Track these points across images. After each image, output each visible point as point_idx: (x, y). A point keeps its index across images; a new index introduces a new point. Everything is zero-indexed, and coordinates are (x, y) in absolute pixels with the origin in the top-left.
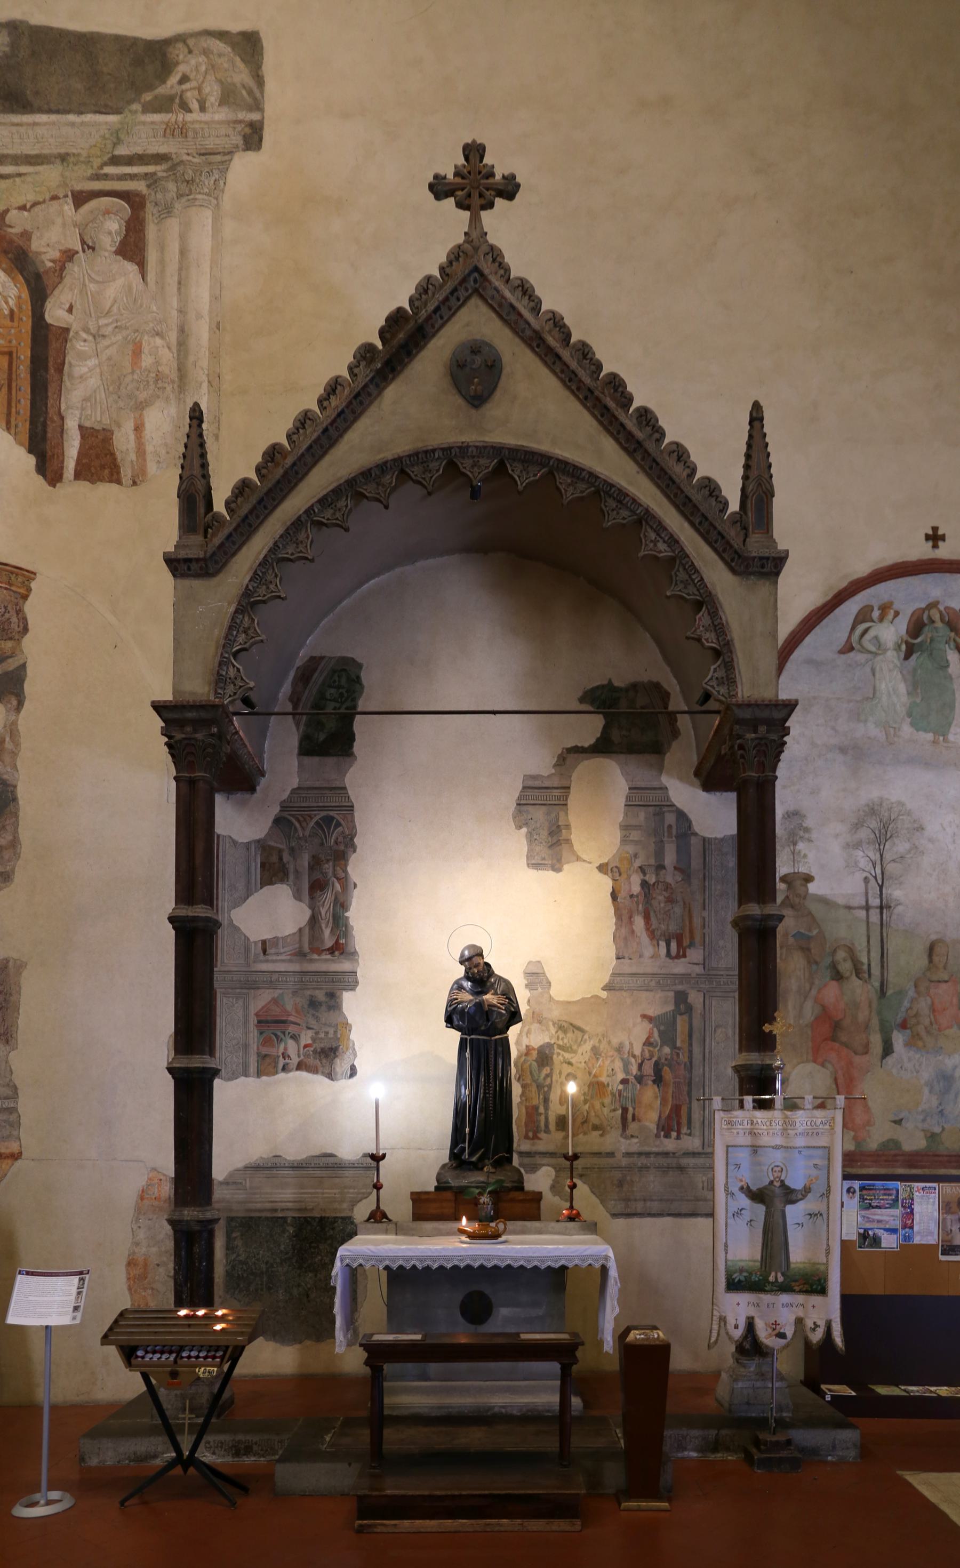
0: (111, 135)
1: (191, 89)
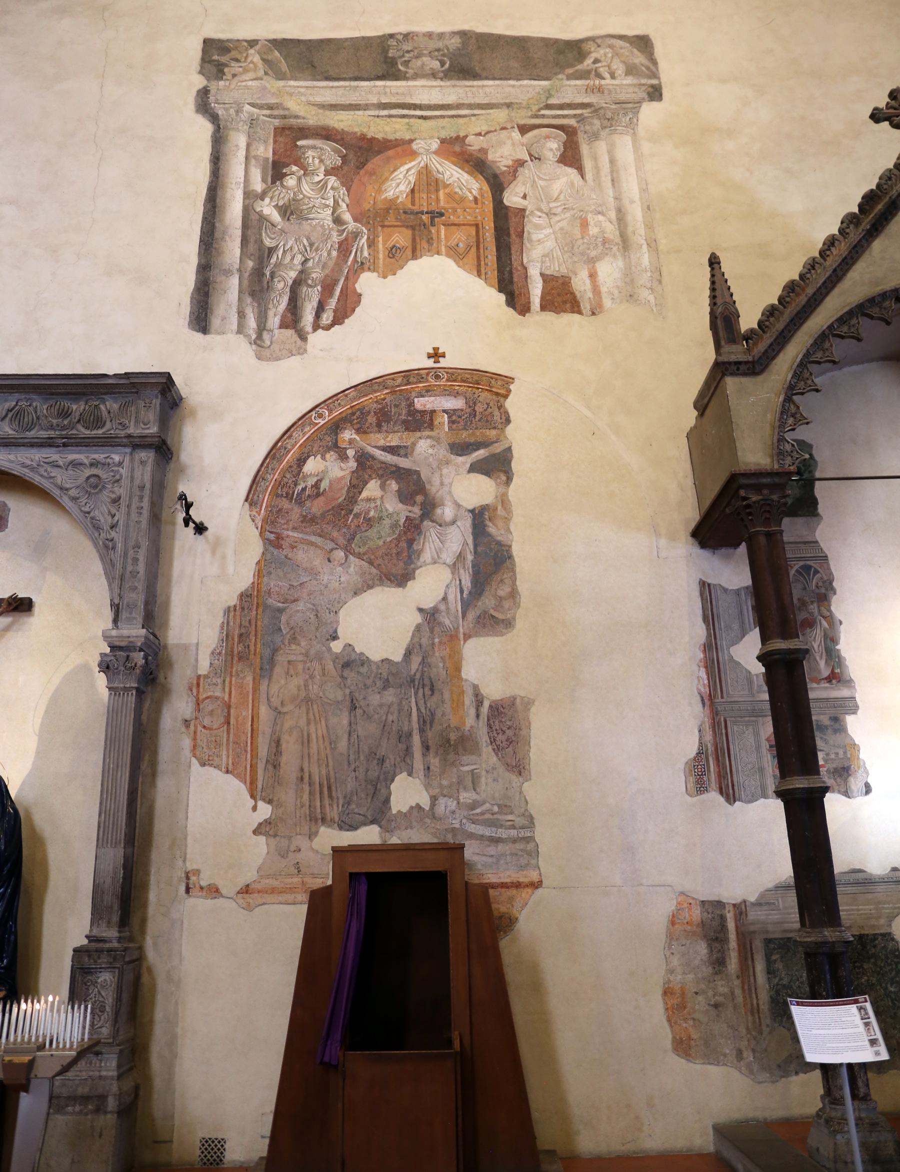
0: (545, 92)
1: (602, 66)
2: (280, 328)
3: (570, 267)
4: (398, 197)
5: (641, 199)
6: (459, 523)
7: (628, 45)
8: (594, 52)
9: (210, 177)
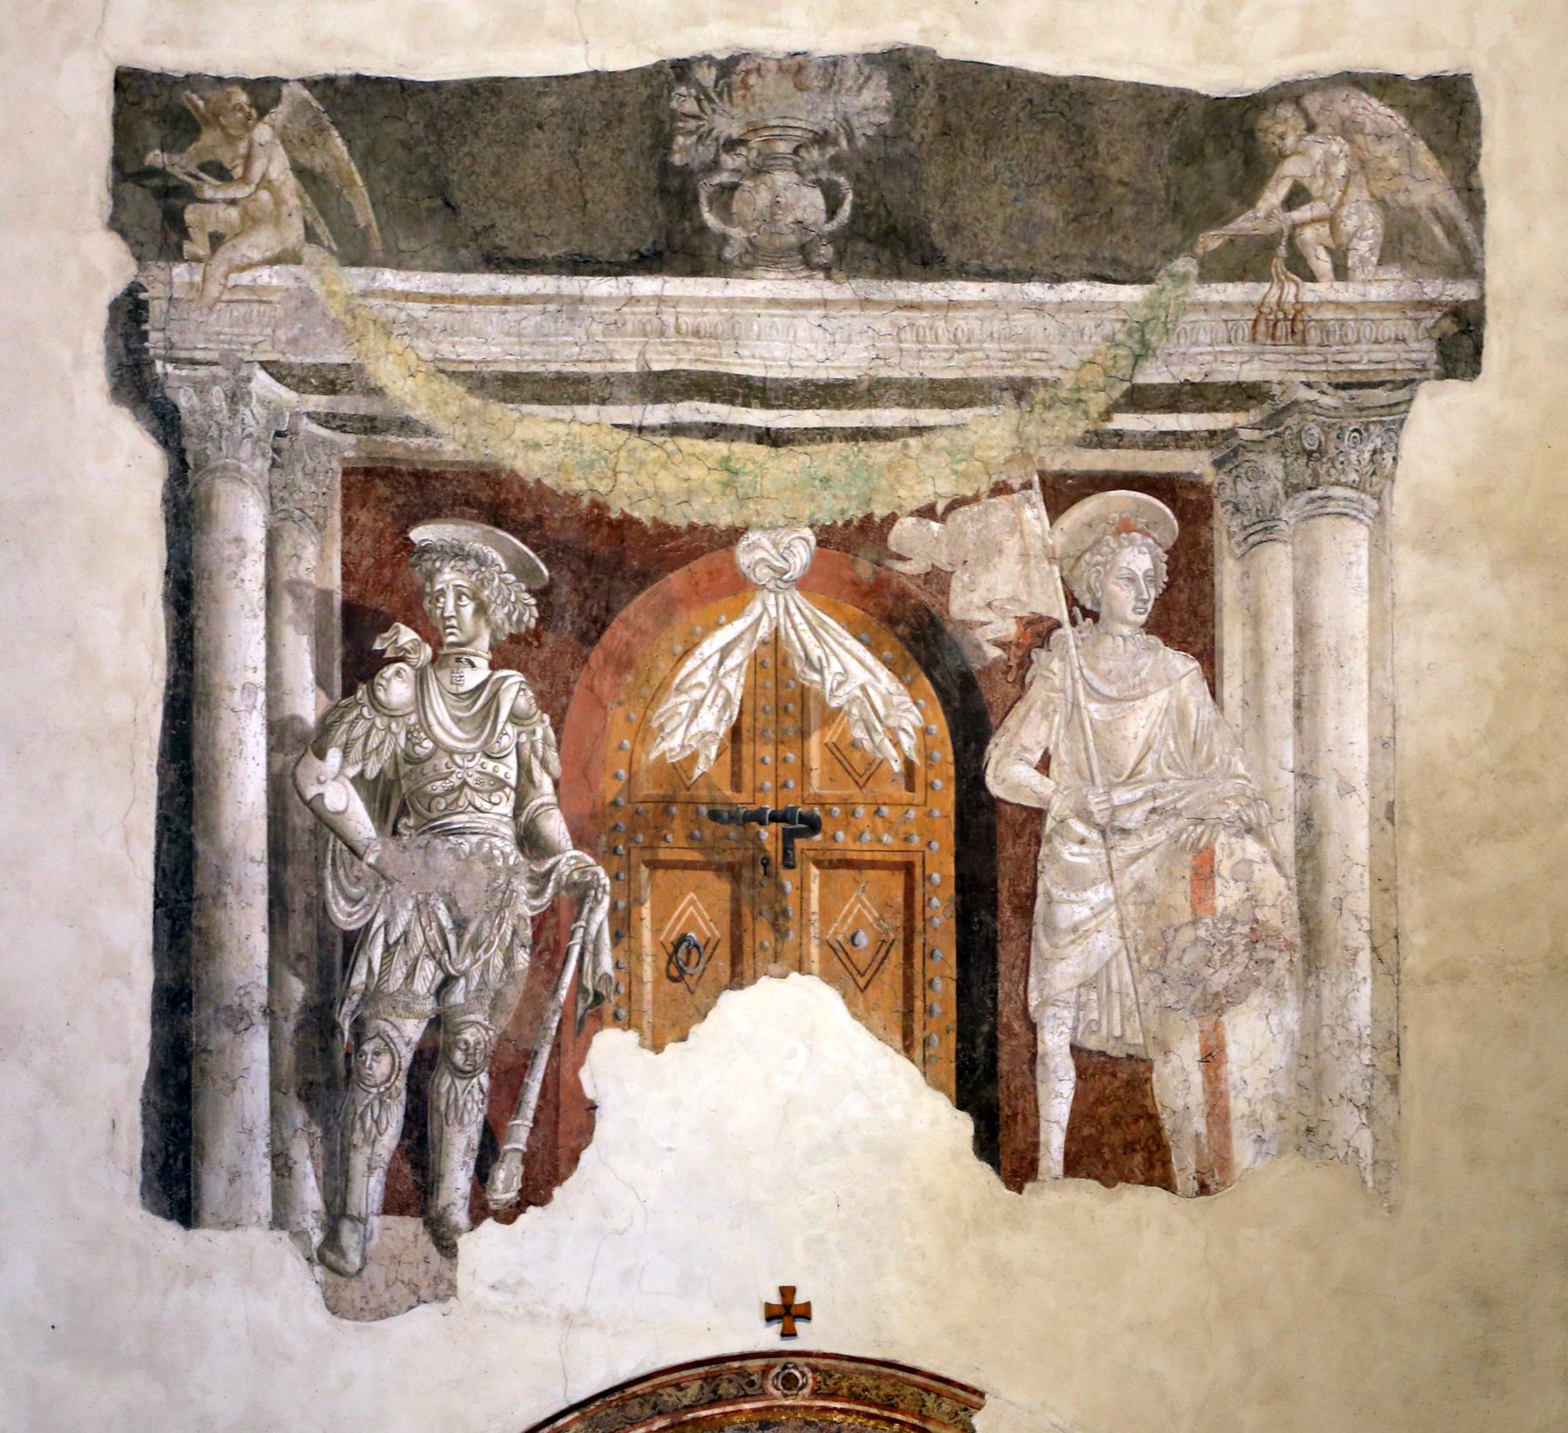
0: (1130, 334)
1: (1313, 221)
2: (386, 1211)
3: (1154, 1027)
4: (694, 758)
5: (1372, 779)
7: (1401, 121)
8: (1295, 153)
9: (170, 661)
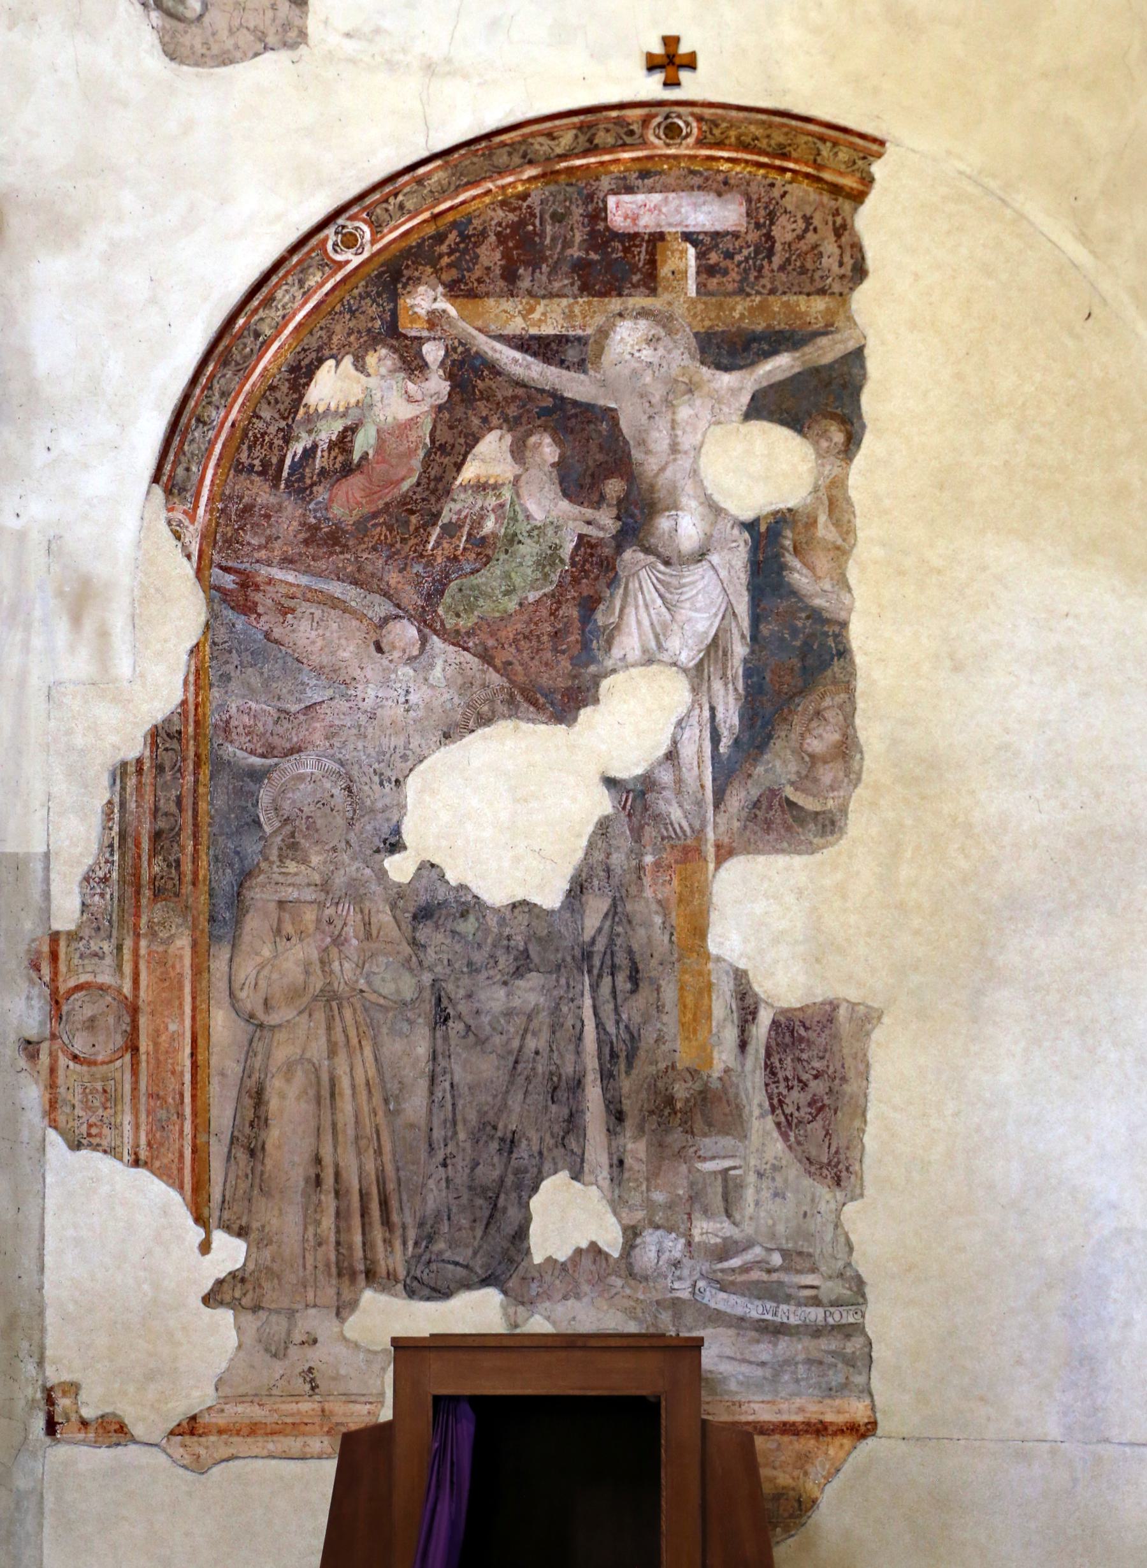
6: (715, 558)
